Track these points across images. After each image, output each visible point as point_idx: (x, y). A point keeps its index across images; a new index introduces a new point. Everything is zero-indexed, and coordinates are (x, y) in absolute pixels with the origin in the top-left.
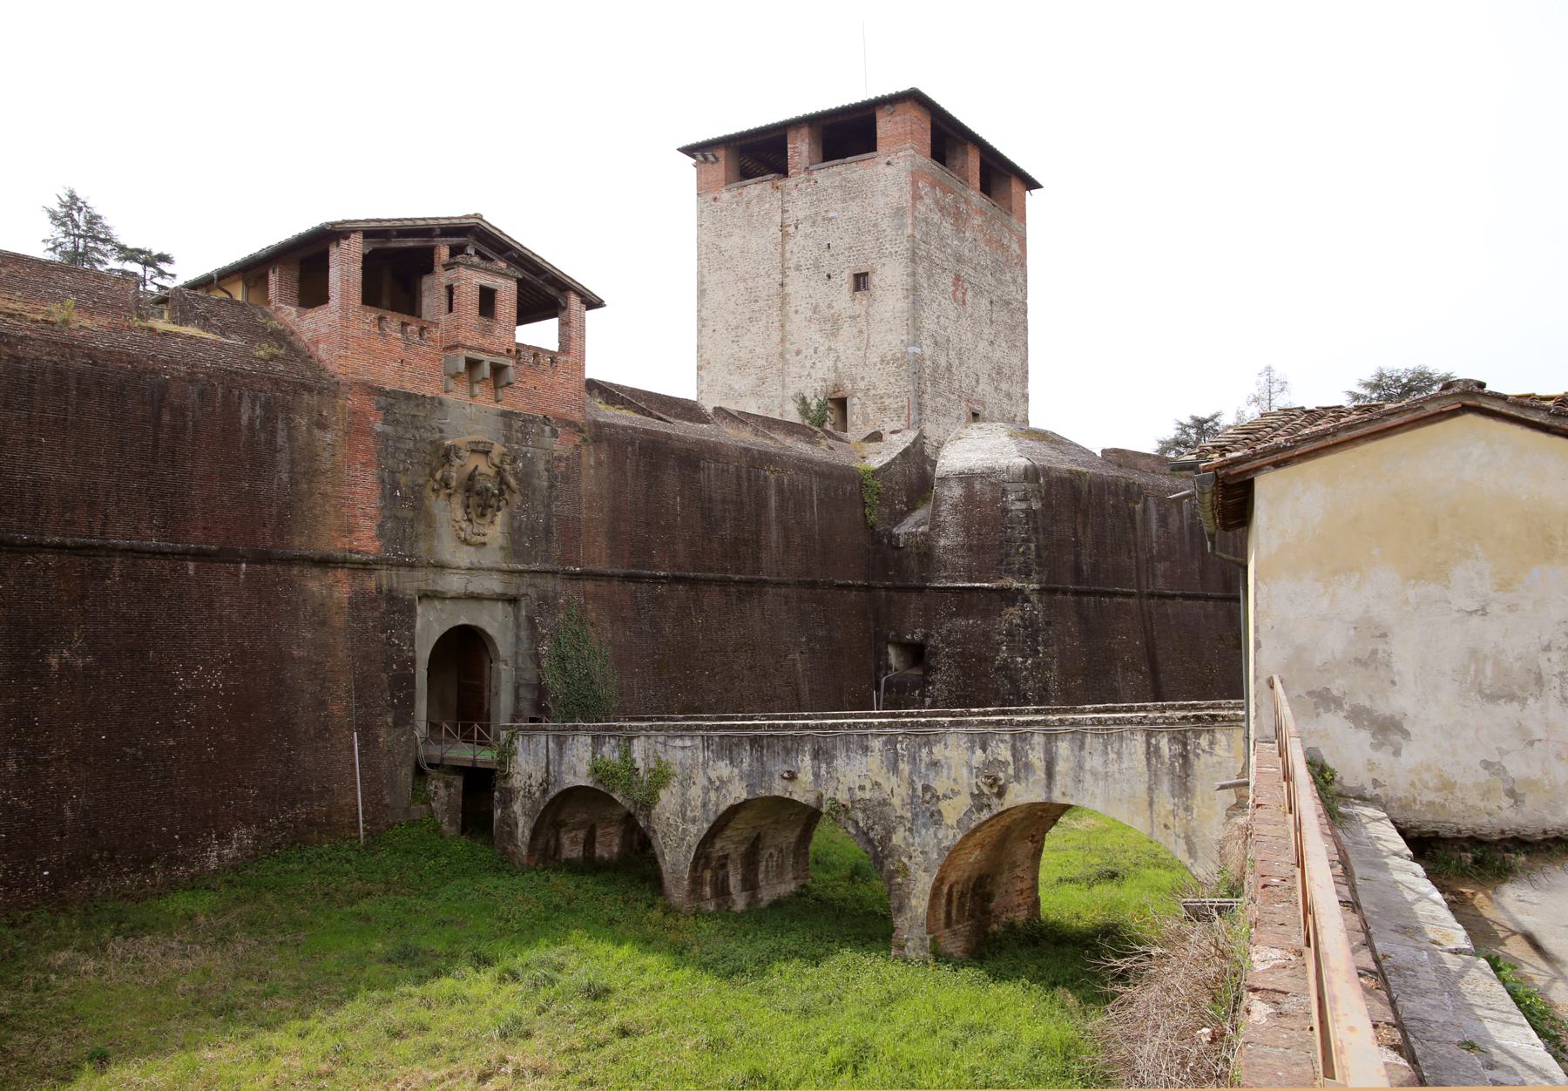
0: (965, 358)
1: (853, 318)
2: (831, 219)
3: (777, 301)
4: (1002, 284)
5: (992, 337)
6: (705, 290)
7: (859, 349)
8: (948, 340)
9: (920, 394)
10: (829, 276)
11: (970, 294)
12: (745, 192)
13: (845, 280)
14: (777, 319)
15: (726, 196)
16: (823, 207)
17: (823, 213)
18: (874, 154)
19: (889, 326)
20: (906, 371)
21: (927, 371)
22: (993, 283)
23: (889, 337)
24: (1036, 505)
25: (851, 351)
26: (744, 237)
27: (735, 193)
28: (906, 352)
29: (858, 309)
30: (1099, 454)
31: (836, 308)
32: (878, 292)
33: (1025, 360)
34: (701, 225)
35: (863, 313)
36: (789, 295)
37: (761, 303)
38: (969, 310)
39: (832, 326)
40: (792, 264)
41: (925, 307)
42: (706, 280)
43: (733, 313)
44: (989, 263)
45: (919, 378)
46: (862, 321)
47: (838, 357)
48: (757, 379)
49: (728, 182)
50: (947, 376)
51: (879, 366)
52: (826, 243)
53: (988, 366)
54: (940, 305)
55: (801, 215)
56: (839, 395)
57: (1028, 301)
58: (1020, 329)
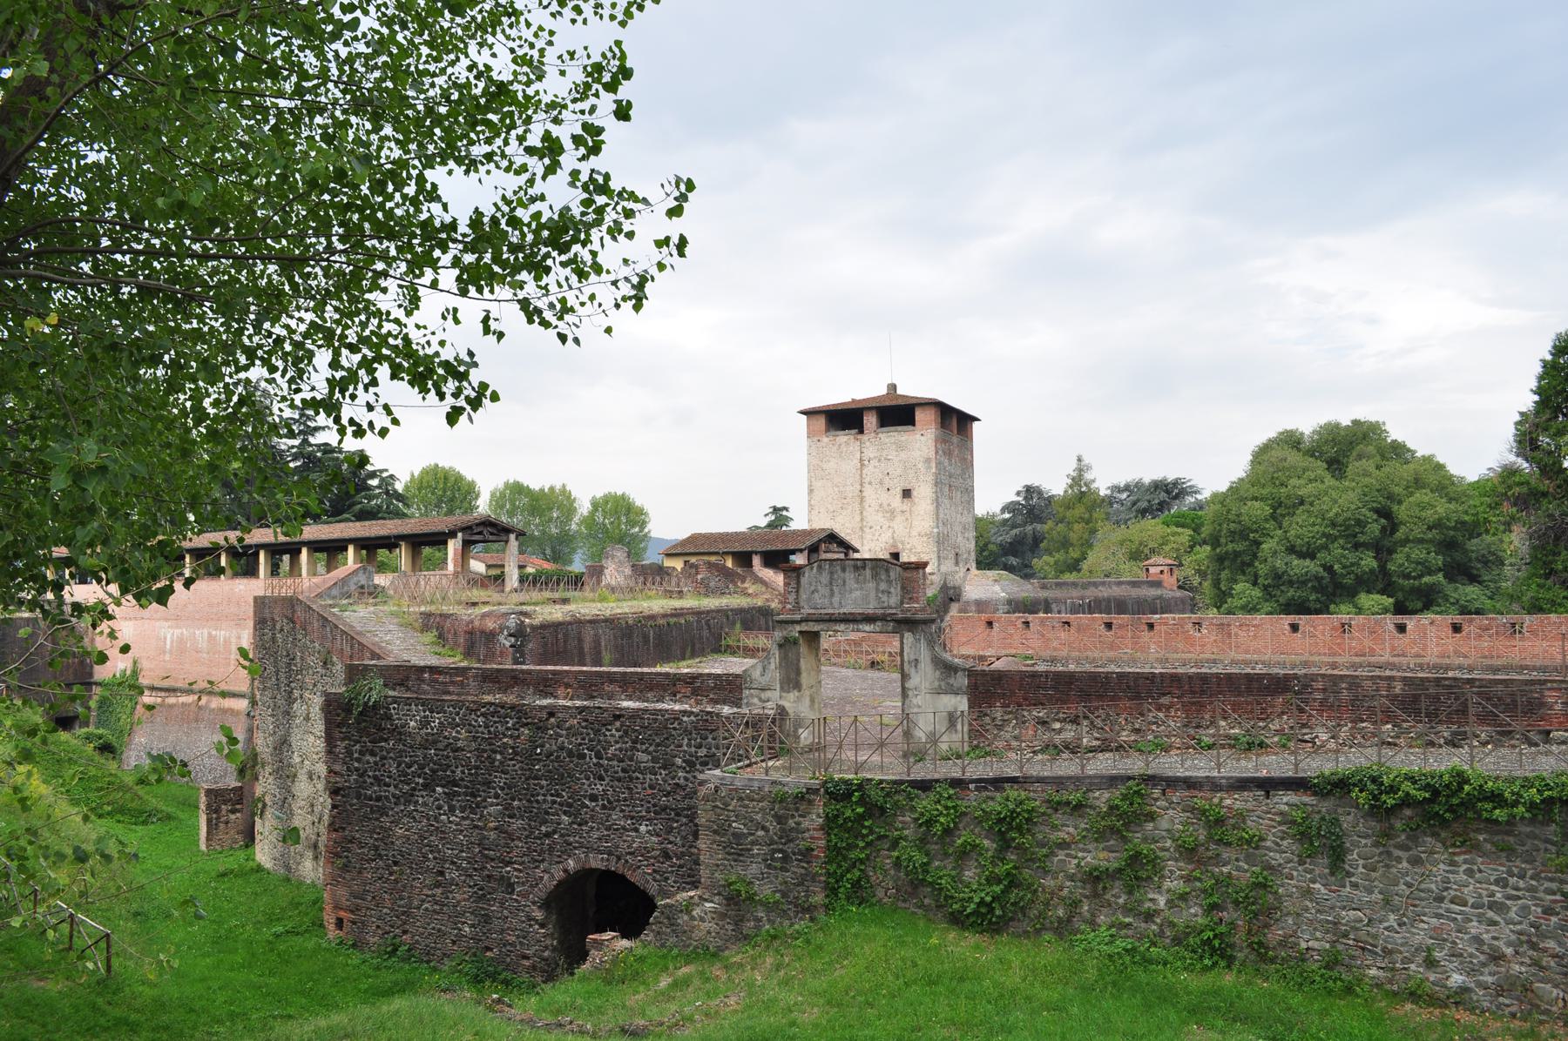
3: (858, 500)
9: (939, 551)
13: (898, 492)
15: (825, 439)
18: (910, 427)
39: (892, 514)
40: (867, 480)
49: (827, 430)
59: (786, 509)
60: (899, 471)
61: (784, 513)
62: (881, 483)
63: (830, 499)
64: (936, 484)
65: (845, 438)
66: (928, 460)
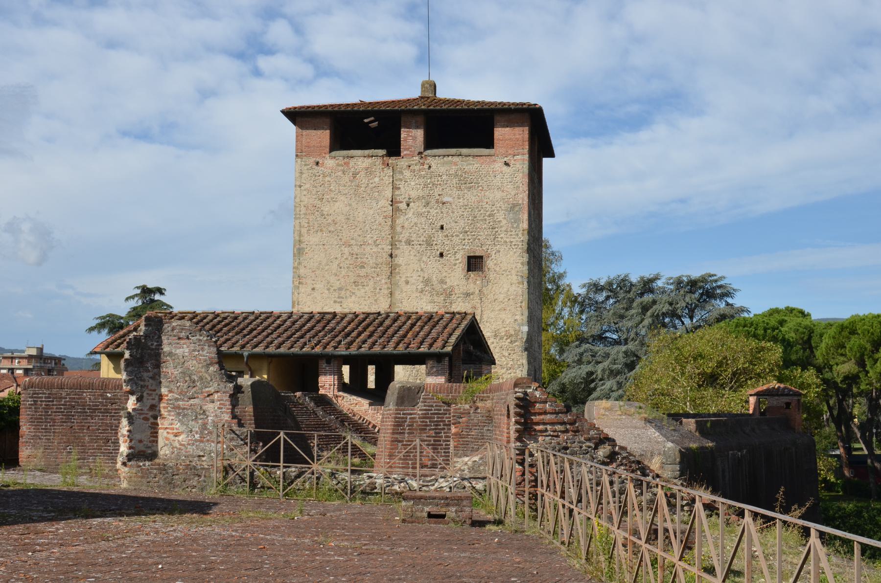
1: (468, 295)
2: (444, 203)
3: (386, 270)
10: (441, 255)
12: (351, 165)
14: (386, 286)
15: (331, 162)
16: (437, 191)
23: (503, 315)
26: (350, 205)
32: (492, 276)
34: (300, 186)
35: (477, 292)
36: (400, 266)
40: (404, 236)
42: (306, 238)
43: (336, 275)
49: (332, 148)
55: (414, 194)
59: (160, 291)
60: (462, 223)
61: (157, 297)
62: (429, 243)
63: (334, 266)
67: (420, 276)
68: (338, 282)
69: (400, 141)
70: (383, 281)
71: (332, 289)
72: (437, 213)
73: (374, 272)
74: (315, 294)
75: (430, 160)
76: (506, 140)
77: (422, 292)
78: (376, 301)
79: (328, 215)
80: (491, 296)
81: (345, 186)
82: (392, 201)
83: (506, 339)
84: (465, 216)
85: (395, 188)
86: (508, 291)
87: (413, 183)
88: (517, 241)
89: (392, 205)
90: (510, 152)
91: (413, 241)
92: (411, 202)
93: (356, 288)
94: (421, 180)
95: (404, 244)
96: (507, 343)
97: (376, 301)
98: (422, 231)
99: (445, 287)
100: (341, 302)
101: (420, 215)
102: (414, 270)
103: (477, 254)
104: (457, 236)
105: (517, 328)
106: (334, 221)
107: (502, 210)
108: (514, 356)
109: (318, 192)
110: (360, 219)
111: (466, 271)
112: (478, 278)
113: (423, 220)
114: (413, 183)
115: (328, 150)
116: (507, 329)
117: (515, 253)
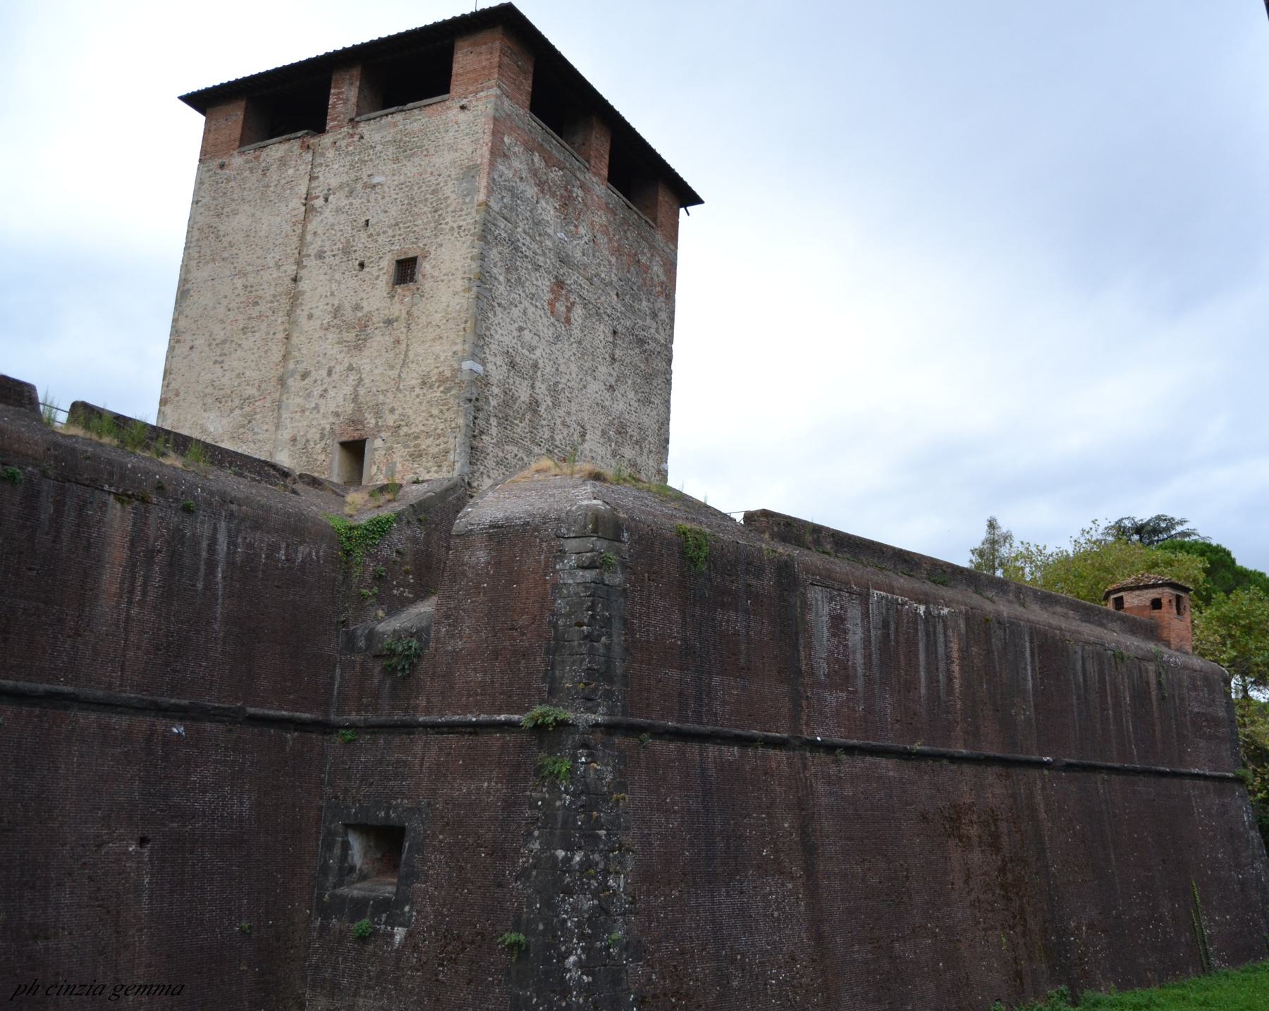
0: (562, 398)
1: (389, 322)
3: (285, 301)
4: (634, 312)
5: (612, 381)
6: (188, 290)
7: (392, 367)
8: (535, 366)
9: (474, 435)
10: (362, 265)
11: (578, 312)
14: (281, 328)
15: (237, 160)
16: (366, 171)
17: (365, 179)
19: (438, 331)
20: (456, 397)
21: (493, 402)
22: (619, 306)
23: (437, 348)
24: (616, 579)
25: (380, 370)
27: (251, 155)
28: (460, 370)
29: (397, 309)
30: (739, 518)
31: (366, 309)
32: (427, 285)
33: (664, 423)
36: (305, 292)
37: (263, 307)
38: (576, 332)
40: (312, 250)
41: (498, 310)
43: (222, 321)
44: (615, 279)
45: (478, 410)
46: (400, 327)
47: (361, 380)
48: (242, 416)
50: (528, 416)
51: (417, 390)
52: (364, 219)
53: (602, 420)
54: (525, 313)
55: (334, 182)
56: (356, 435)
57: (674, 346)
58: (659, 381)
60: (394, 211)
63: (221, 310)
64: (485, 234)
65: (285, 147)
66: (470, 172)
67: (327, 304)
68: (222, 333)
69: (328, 108)
70: (280, 320)
71: (214, 343)
72: (362, 202)
73: (270, 308)
74: (194, 355)
75: (364, 128)
76: (468, 72)
77: (326, 329)
78: (266, 352)
79: (224, 236)
80: (423, 320)
81: (250, 189)
82: (306, 199)
83: (438, 387)
84: (398, 201)
85: (312, 178)
86: (448, 306)
87: (336, 166)
88: (468, 224)
89: (305, 205)
90: (471, 89)
91: (326, 252)
92: (330, 195)
93: (244, 337)
94: (349, 158)
95: (312, 257)
96: (438, 394)
97: (266, 352)
98: (339, 234)
99: (360, 314)
100: (222, 362)
101: (338, 210)
102: (321, 296)
103: (410, 255)
104: (384, 232)
105: (456, 366)
106: (230, 242)
107: (451, 180)
108: (448, 415)
109: (217, 205)
110: (263, 234)
111: (390, 285)
112: (407, 293)
113: (343, 217)
114: (336, 166)
115: (238, 143)
116: (441, 369)
117: (464, 243)
